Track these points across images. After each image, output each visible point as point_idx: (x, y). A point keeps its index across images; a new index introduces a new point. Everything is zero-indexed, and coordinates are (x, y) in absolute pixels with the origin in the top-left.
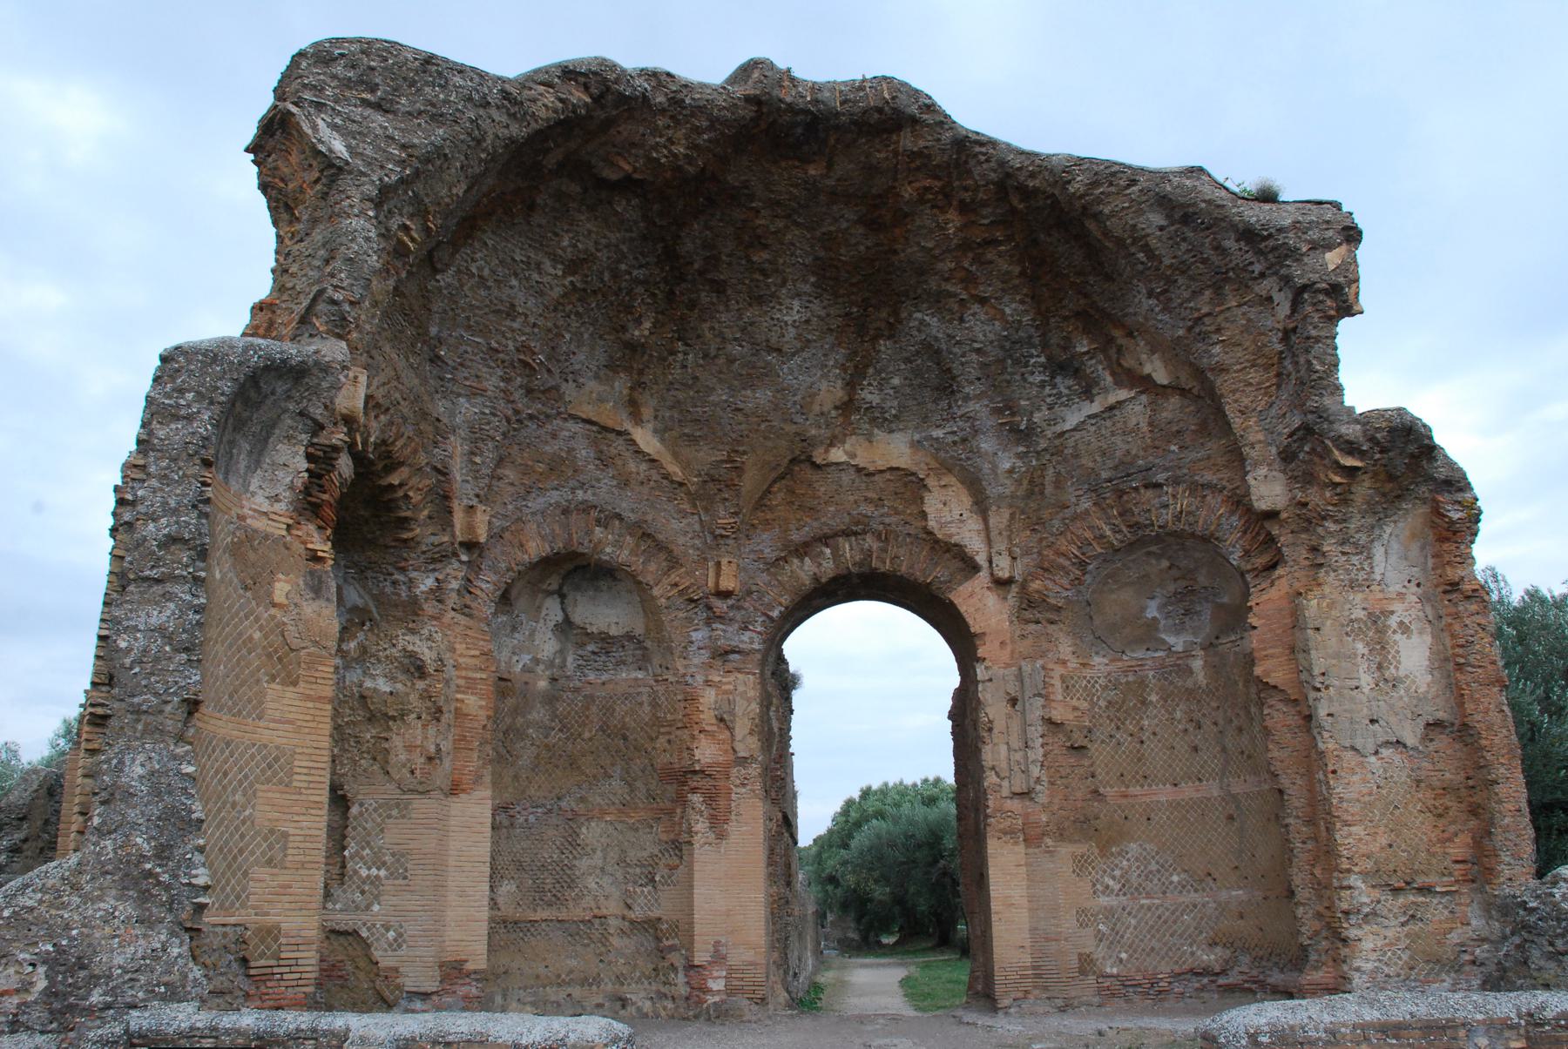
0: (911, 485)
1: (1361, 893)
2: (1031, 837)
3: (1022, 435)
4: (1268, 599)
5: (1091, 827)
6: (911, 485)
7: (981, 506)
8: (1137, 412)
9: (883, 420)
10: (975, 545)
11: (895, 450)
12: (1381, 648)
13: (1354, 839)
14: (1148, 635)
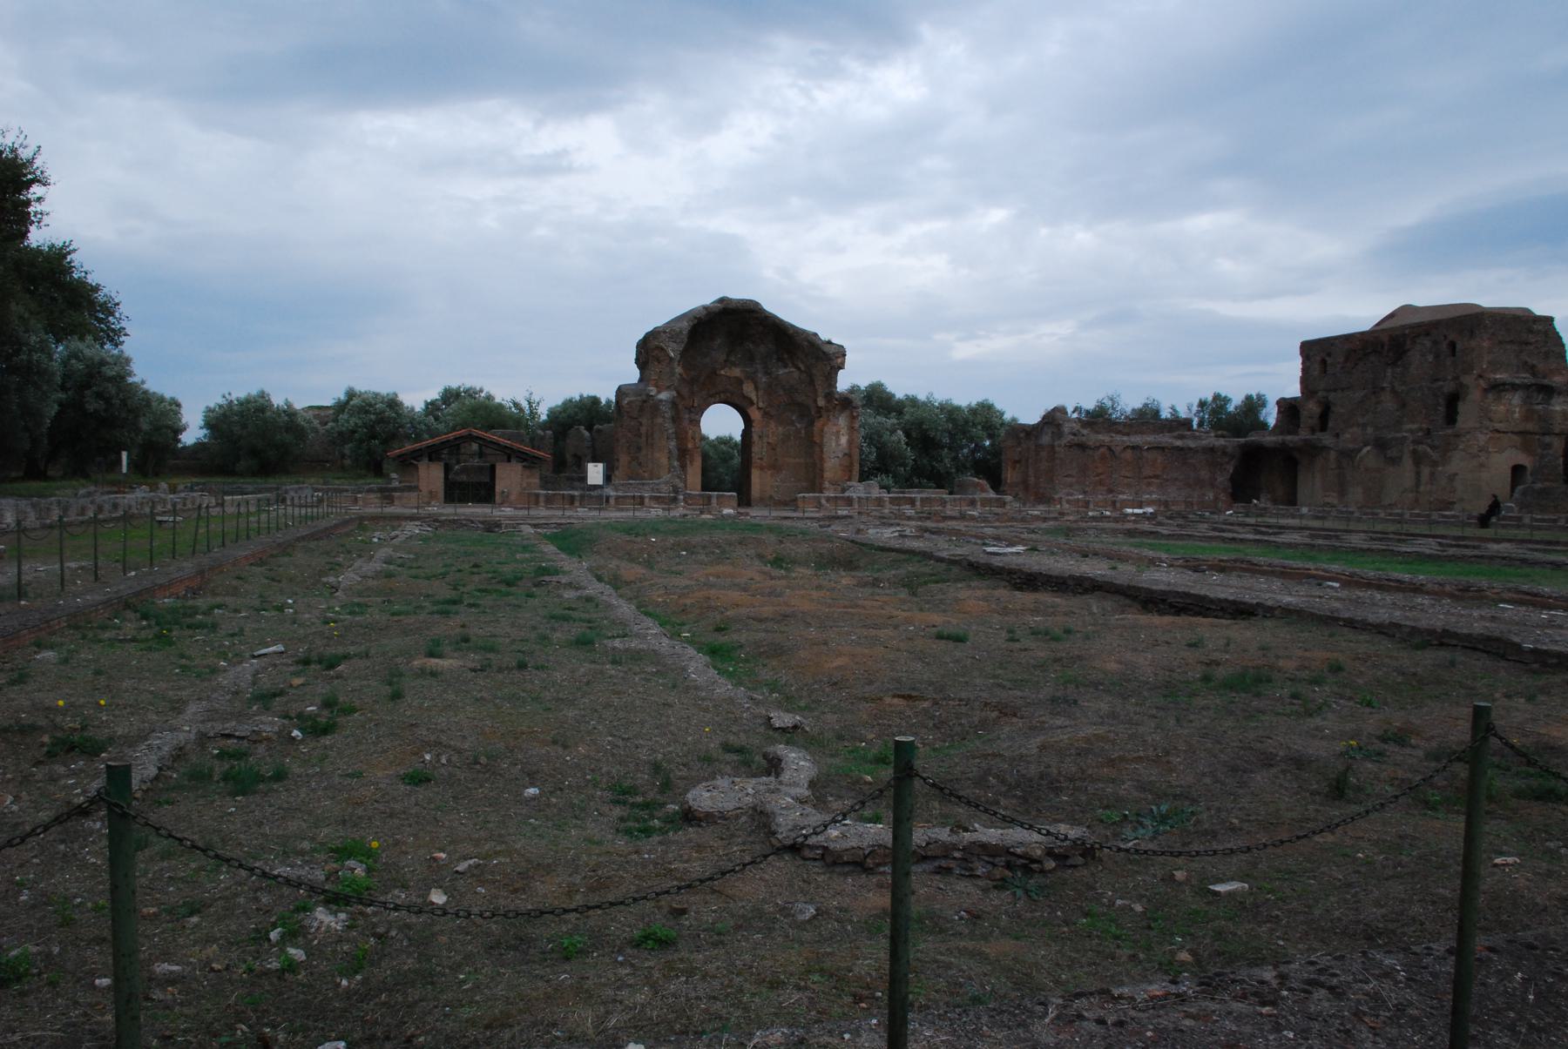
0: (739, 382)
1: (827, 484)
2: (762, 468)
3: (767, 373)
4: (818, 424)
5: (775, 467)
6: (739, 382)
7: (757, 388)
8: (796, 374)
9: (734, 364)
10: (754, 398)
11: (737, 372)
12: (838, 438)
13: (827, 475)
14: (792, 423)
